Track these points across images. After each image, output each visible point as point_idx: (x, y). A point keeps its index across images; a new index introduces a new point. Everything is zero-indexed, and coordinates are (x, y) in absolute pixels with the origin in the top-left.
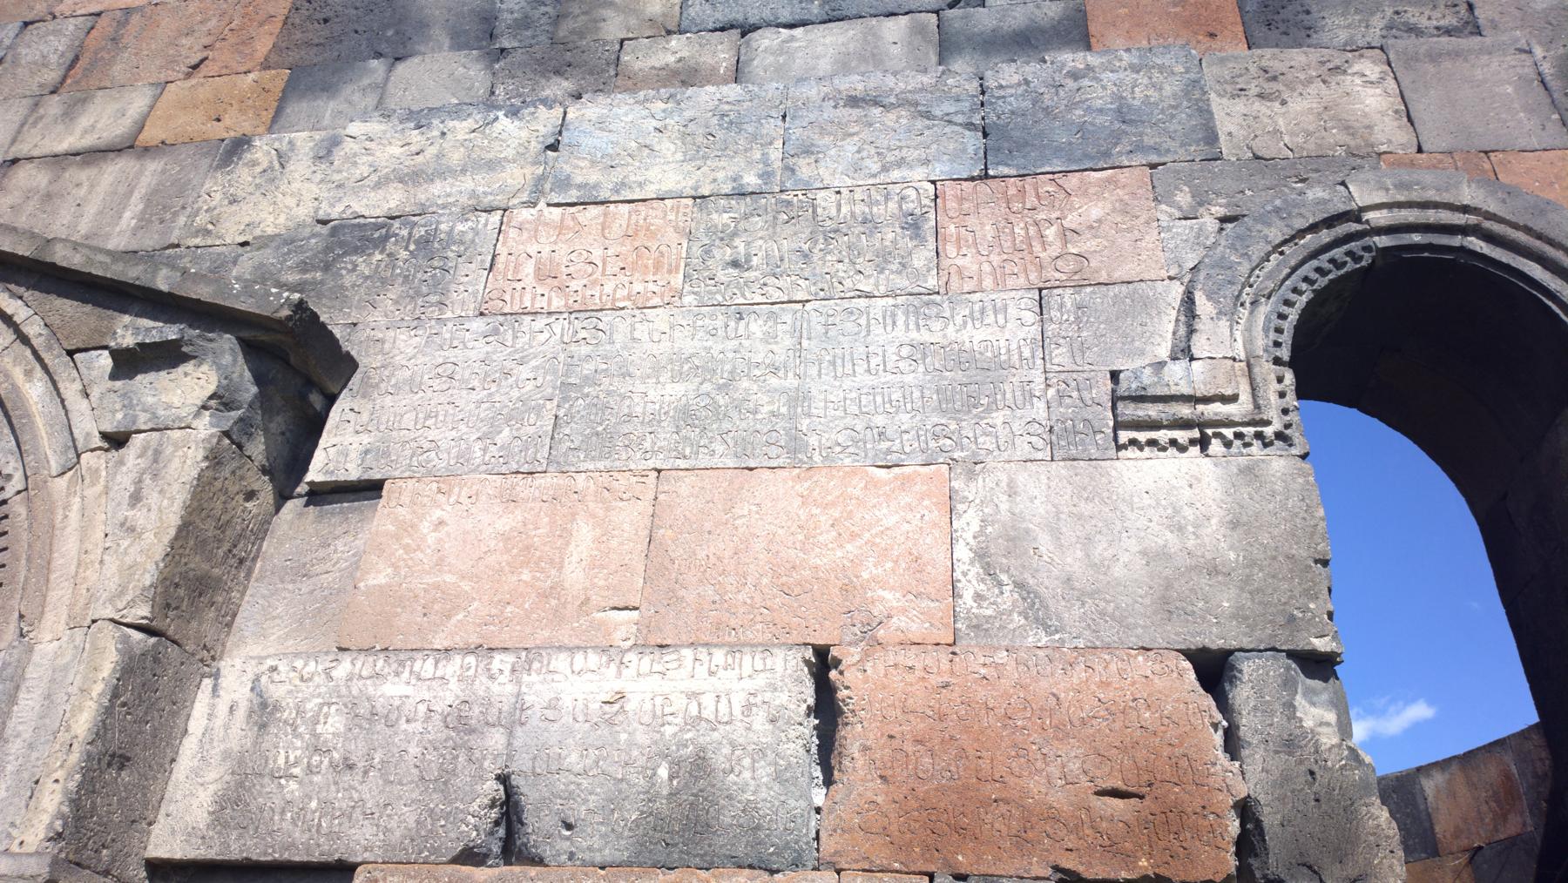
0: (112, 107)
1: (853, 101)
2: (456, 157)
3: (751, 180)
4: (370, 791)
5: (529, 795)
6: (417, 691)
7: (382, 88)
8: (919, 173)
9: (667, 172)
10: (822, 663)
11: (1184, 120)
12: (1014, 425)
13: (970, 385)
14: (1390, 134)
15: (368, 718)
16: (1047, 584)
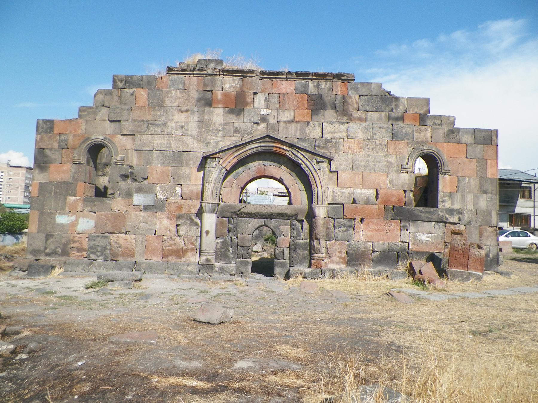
0: (289, 113)
1: (380, 128)
2: (337, 130)
3: (369, 138)
4: (344, 198)
5: (356, 199)
6: (346, 191)
7: (324, 115)
8: (386, 139)
9: (360, 136)
10: (377, 190)
11: (411, 136)
12: (393, 169)
13: (389, 165)
14: (429, 140)
15: (342, 193)
16: (394, 184)
